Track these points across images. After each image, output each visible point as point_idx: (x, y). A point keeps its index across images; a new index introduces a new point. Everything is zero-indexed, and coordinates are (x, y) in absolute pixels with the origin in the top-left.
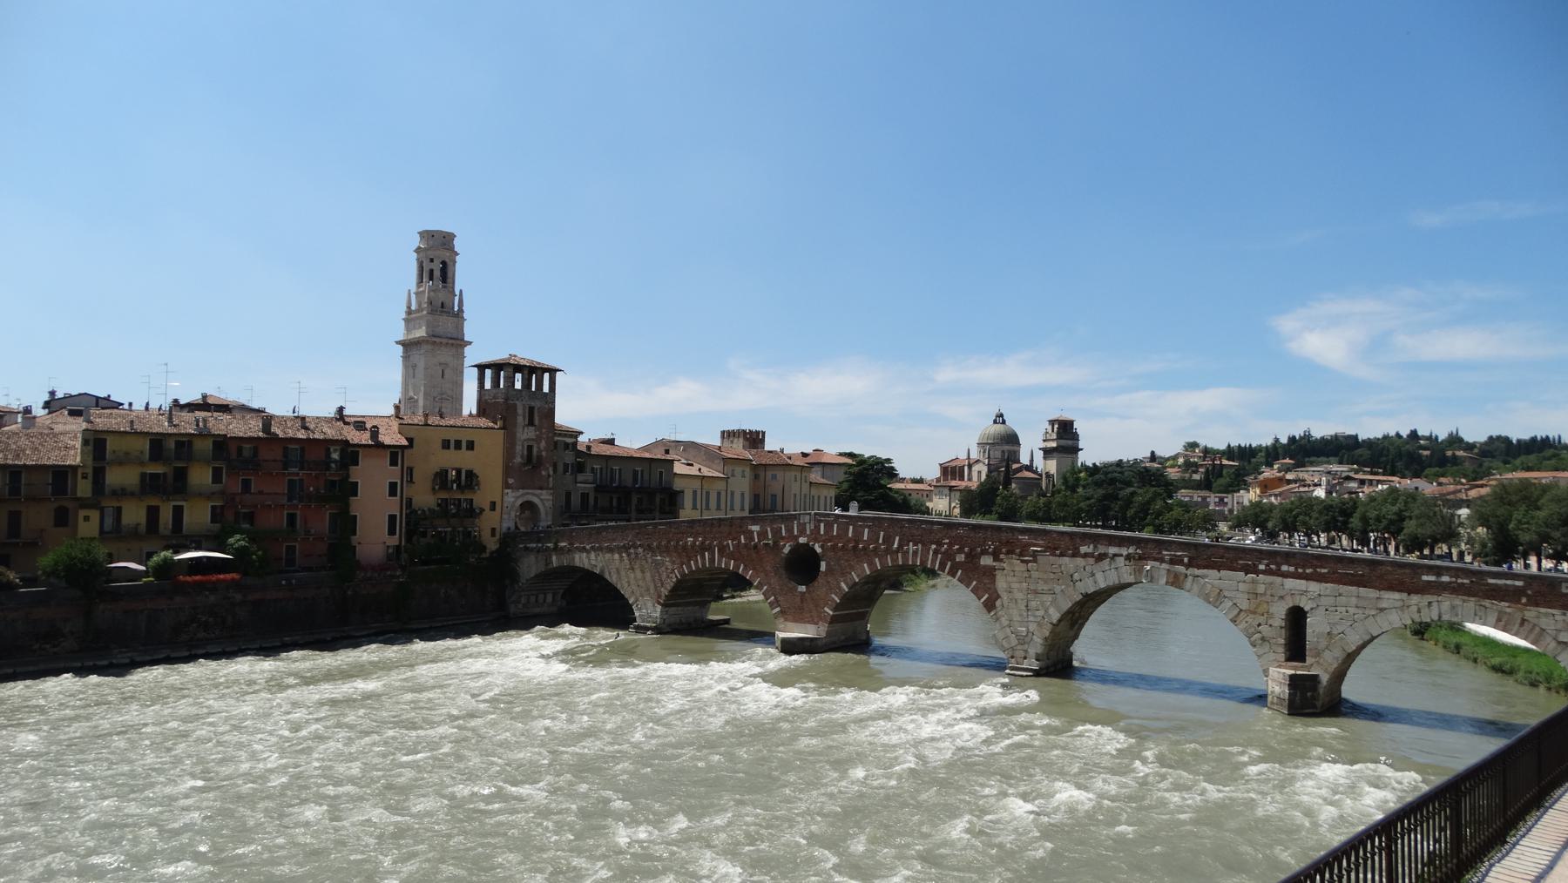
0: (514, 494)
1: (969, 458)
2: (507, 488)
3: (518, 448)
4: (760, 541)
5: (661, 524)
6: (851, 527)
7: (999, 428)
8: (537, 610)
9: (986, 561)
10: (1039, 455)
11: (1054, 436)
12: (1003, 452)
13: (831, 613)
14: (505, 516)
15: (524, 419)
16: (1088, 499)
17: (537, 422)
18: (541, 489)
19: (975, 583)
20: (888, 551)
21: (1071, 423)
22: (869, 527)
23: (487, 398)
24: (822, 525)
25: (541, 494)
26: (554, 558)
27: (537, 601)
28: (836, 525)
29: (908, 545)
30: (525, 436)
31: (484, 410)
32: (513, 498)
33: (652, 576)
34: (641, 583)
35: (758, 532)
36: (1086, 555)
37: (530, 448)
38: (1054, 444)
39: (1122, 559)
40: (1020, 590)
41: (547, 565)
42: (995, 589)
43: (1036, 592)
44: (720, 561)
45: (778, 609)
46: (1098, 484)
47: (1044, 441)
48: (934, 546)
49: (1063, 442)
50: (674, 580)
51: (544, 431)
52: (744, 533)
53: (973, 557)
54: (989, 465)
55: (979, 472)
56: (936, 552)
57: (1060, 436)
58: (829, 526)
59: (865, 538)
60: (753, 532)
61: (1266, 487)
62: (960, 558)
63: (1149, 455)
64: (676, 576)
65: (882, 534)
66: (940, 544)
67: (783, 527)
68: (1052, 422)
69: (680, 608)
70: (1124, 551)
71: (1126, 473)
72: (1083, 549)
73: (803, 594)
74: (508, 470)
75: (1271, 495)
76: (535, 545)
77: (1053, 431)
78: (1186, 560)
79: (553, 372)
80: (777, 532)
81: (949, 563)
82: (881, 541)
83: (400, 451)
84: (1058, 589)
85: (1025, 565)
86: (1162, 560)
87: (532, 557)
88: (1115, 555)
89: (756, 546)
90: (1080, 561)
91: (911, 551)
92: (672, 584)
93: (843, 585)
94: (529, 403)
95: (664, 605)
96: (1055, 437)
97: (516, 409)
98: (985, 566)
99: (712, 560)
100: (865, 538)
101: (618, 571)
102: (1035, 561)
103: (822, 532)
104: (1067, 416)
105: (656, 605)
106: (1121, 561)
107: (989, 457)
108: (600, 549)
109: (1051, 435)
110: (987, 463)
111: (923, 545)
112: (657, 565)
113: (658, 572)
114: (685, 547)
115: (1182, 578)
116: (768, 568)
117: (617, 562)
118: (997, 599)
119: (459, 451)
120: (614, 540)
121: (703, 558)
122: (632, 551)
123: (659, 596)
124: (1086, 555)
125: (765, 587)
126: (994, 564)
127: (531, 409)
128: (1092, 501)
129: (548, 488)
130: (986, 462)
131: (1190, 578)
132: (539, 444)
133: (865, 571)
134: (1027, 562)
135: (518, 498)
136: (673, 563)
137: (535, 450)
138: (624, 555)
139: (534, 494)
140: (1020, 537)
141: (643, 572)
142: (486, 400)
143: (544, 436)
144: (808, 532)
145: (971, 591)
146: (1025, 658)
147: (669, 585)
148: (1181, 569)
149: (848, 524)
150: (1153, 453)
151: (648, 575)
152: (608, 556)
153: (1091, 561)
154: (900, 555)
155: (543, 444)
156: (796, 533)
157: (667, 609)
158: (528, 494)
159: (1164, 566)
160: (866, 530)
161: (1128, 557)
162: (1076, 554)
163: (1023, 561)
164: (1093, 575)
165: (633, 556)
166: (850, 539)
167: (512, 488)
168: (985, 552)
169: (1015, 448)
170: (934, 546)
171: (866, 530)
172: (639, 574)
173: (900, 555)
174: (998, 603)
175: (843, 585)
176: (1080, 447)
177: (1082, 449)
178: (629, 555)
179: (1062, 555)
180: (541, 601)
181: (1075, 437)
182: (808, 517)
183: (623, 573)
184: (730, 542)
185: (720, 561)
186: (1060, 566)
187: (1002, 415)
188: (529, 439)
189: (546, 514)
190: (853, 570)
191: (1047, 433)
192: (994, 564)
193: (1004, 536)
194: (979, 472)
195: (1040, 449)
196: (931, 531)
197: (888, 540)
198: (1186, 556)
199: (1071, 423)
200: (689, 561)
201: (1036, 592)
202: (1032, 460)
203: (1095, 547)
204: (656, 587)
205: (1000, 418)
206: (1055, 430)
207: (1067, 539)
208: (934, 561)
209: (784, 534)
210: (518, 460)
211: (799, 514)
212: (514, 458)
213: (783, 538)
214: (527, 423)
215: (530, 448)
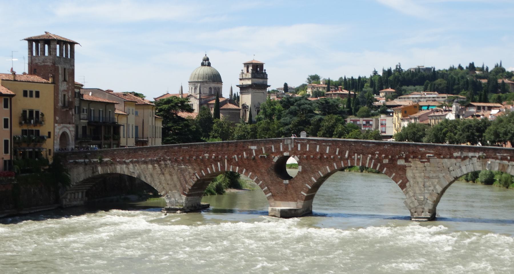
1: (182, 93)
2: (56, 123)
3: (60, 96)
4: (257, 155)
5: (184, 146)
6: (318, 146)
7: (206, 69)
8: (75, 203)
9: (401, 162)
11: (249, 76)
12: (210, 88)
13: (305, 195)
14: (55, 142)
16: (287, 124)
17: (67, 79)
18: (70, 123)
19: (394, 174)
20: (342, 158)
21: (261, 66)
22: (330, 146)
23: (37, 62)
24: (299, 145)
26: (99, 168)
27: (74, 198)
28: (308, 145)
29: (354, 155)
31: (35, 70)
32: (59, 130)
33: (178, 178)
34: (169, 182)
35: (256, 151)
36: (457, 158)
38: (249, 82)
39: (476, 159)
40: (420, 177)
41: (93, 173)
42: (406, 177)
43: (429, 178)
44: (228, 167)
45: (270, 194)
46: (294, 113)
47: (241, 79)
48: (370, 156)
49: (257, 81)
50: (196, 179)
52: (245, 150)
53: (393, 161)
54: (200, 99)
56: (371, 159)
57: (254, 76)
58: (303, 146)
59: (327, 152)
60: (252, 150)
61: (405, 112)
62: (386, 161)
63: (283, 86)
64: (197, 178)
65: (338, 149)
66: (373, 154)
67: (273, 147)
68: (247, 65)
70: (477, 155)
71: (313, 105)
72: (455, 154)
73: (286, 185)
74: (56, 111)
75: (411, 119)
76: (82, 160)
77: (248, 71)
78: (509, 158)
79: (72, 44)
80: (269, 150)
81: (379, 165)
82: (337, 153)
83: (9, 98)
84: (441, 175)
85: (423, 163)
86: (496, 158)
87: (81, 169)
88: (472, 157)
89: (254, 158)
90: (453, 161)
91: (356, 159)
92: (194, 182)
93: (313, 179)
94: (64, 66)
95: (188, 195)
96: (250, 77)
98: (400, 165)
99: (223, 167)
100: (327, 152)
101: (152, 175)
102: (429, 161)
103: (299, 149)
104: (258, 60)
105: (182, 195)
106: (475, 160)
107: (200, 93)
108: (138, 162)
109: (246, 75)
110: (198, 97)
111: (363, 155)
112: (182, 171)
113: (183, 175)
114: (203, 160)
115: (506, 167)
116: (263, 171)
117: (151, 170)
118: (406, 182)
119: (32, 98)
120: (148, 156)
121: (216, 166)
122: (162, 162)
123: (184, 190)
124: (457, 158)
125: (261, 182)
126: (406, 164)
128: (291, 126)
131: (510, 167)
132: (68, 93)
133: (327, 170)
134: (424, 162)
136: (194, 169)
137: (67, 97)
138: (156, 165)
139: (66, 127)
140: (420, 149)
141: (171, 175)
142: (37, 63)
143: (71, 88)
144: (290, 149)
145: (392, 179)
146: (423, 212)
147: (192, 182)
148: (506, 162)
149: (316, 144)
150: (286, 85)
151: (175, 177)
152: (143, 166)
153: (459, 160)
154: (349, 161)
155: (70, 94)
156: (281, 150)
158: (64, 127)
159: (498, 161)
160: (328, 148)
161: (479, 158)
162: (451, 157)
163: (422, 162)
164: (460, 167)
165: (163, 166)
166: (318, 153)
168: (400, 158)
169: (218, 85)
170: (370, 156)
171: (328, 148)
172: (168, 177)
173: (349, 161)
174: (407, 184)
175: (313, 179)
177: (269, 86)
178: (160, 165)
179: (444, 158)
180: (76, 197)
181: (264, 76)
182: (290, 140)
183: (156, 176)
184: (236, 156)
185: (228, 167)
186: (442, 164)
187: (207, 59)
188: (64, 91)
190: (320, 170)
191: (243, 73)
192: (406, 164)
193: (411, 149)
195: (237, 86)
196: (368, 147)
197: (342, 153)
198: (508, 156)
199: (261, 66)
200: (206, 168)
201: (429, 178)
203: (462, 153)
204: (181, 184)
205: (206, 63)
206: (250, 70)
207: (446, 149)
208: (370, 164)
209: (273, 151)
211: (284, 139)
213: (273, 153)
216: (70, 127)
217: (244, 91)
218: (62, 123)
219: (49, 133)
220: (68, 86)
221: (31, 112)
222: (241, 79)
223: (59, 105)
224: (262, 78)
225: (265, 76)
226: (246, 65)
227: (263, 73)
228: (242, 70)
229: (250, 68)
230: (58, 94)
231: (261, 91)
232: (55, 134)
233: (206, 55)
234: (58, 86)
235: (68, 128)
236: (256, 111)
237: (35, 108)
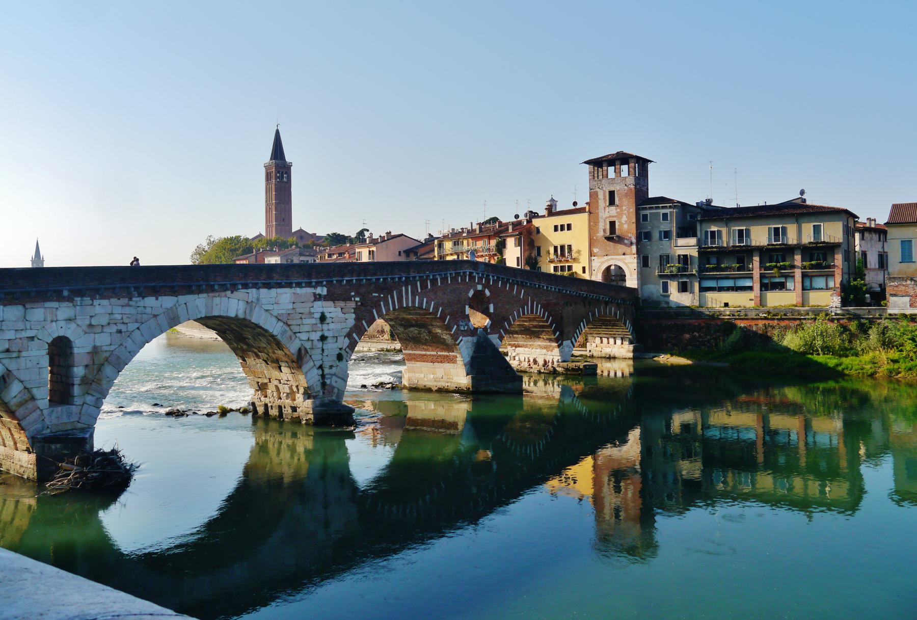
0: (600, 260)
15: (605, 203)
18: (624, 254)
25: (625, 259)
30: (607, 215)
37: (612, 224)
51: (624, 208)
69: (526, 349)
97: (597, 196)
127: (612, 194)
129: (631, 254)
135: (603, 263)
139: (616, 259)
143: (626, 212)
155: (624, 218)
157: (514, 348)
158: (612, 259)
167: (598, 256)
188: (610, 217)
189: (631, 275)
210: (601, 233)
212: (598, 233)
214: (608, 204)
215: (612, 224)
216: (625, 259)
218: (607, 255)
219: (584, 268)
220: (618, 210)
221: (562, 247)
223: (599, 234)
230: (597, 223)
232: (593, 269)
234: (598, 214)
235: (619, 260)
237: (566, 243)
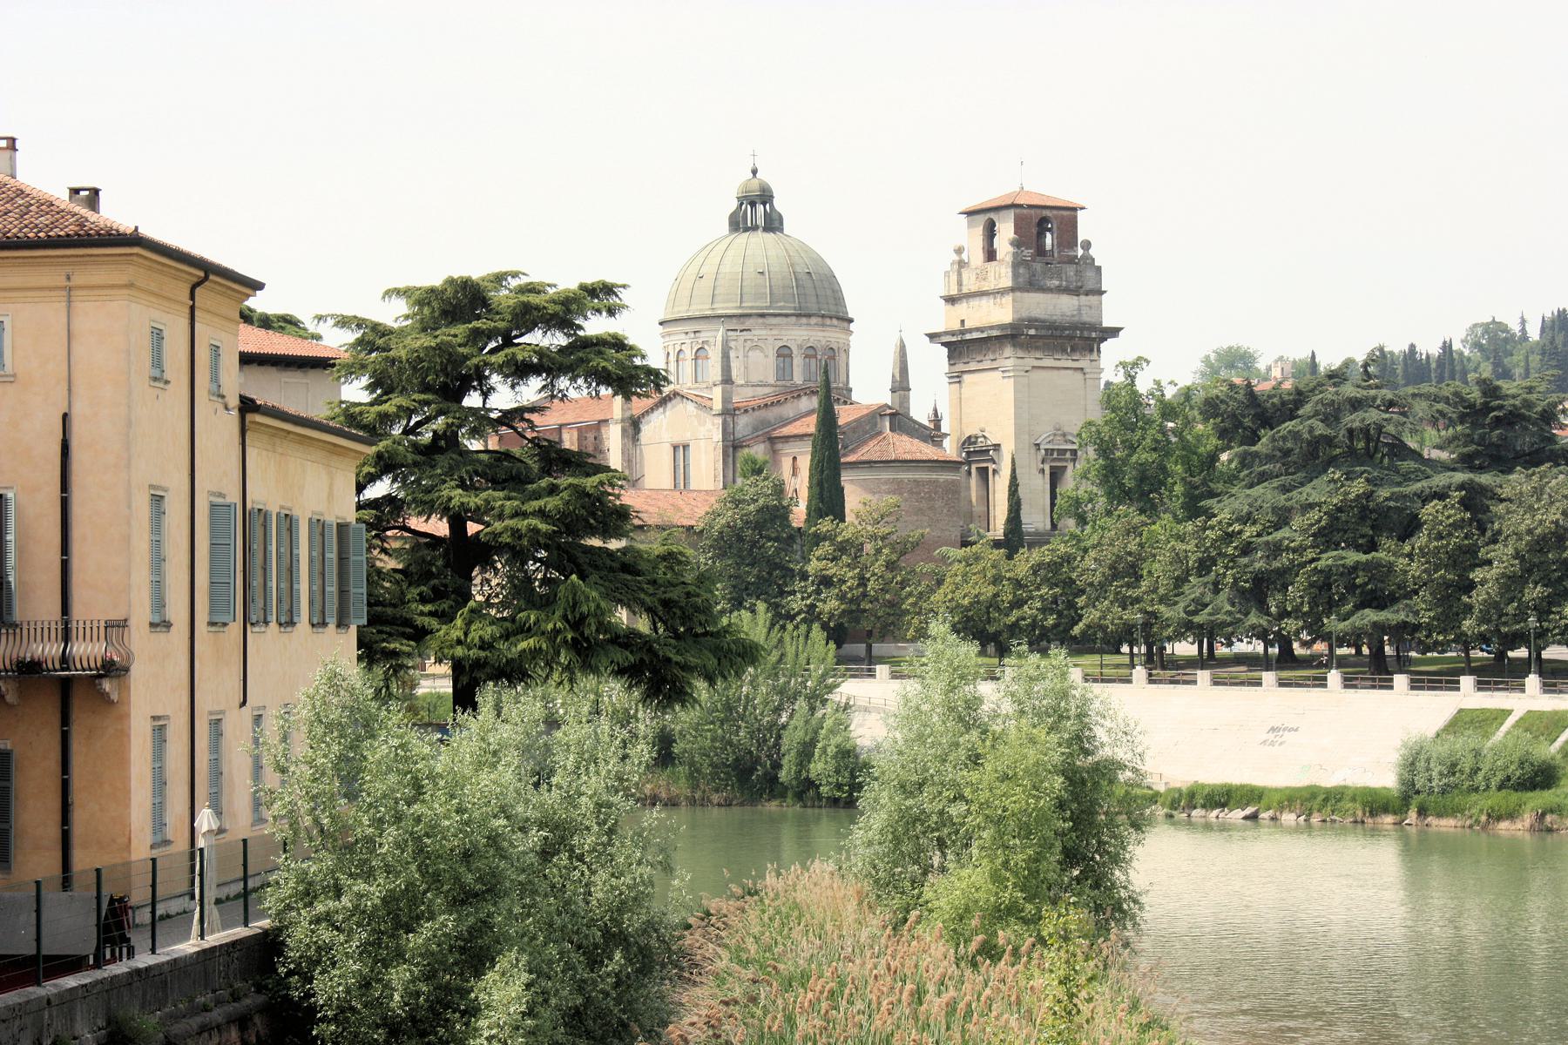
7: (759, 241)
10: (930, 364)
11: (1002, 274)
12: (784, 353)
38: (1000, 313)
47: (951, 300)
54: (729, 412)
55: (680, 450)
57: (1027, 282)
68: (985, 217)
77: (991, 255)
96: (1007, 282)
104: (1050, 188)
107: (727, 380)
109: (982, 276)
110: (718, 406)
130: (717, 394)
176: (1107, 322)
177: (1115, 332)
187: (765, 196)
194: (680, 450)
195: (933, 337)
202: (901, 386)
217: (973, 366)
222: (951, 300)
224: (1075, 291)
225: (1090, 274)
226: (983, 218)
227: (1072, 260)
228: (959, 251)
229: (1006, 231)
231: (1070, 364)
233: (754, 172)
236: (1042, 471)
